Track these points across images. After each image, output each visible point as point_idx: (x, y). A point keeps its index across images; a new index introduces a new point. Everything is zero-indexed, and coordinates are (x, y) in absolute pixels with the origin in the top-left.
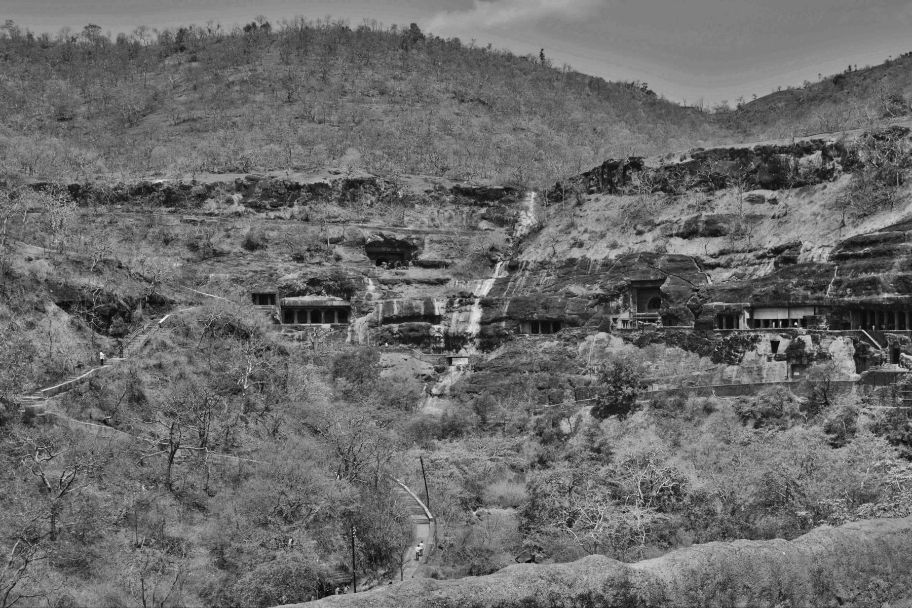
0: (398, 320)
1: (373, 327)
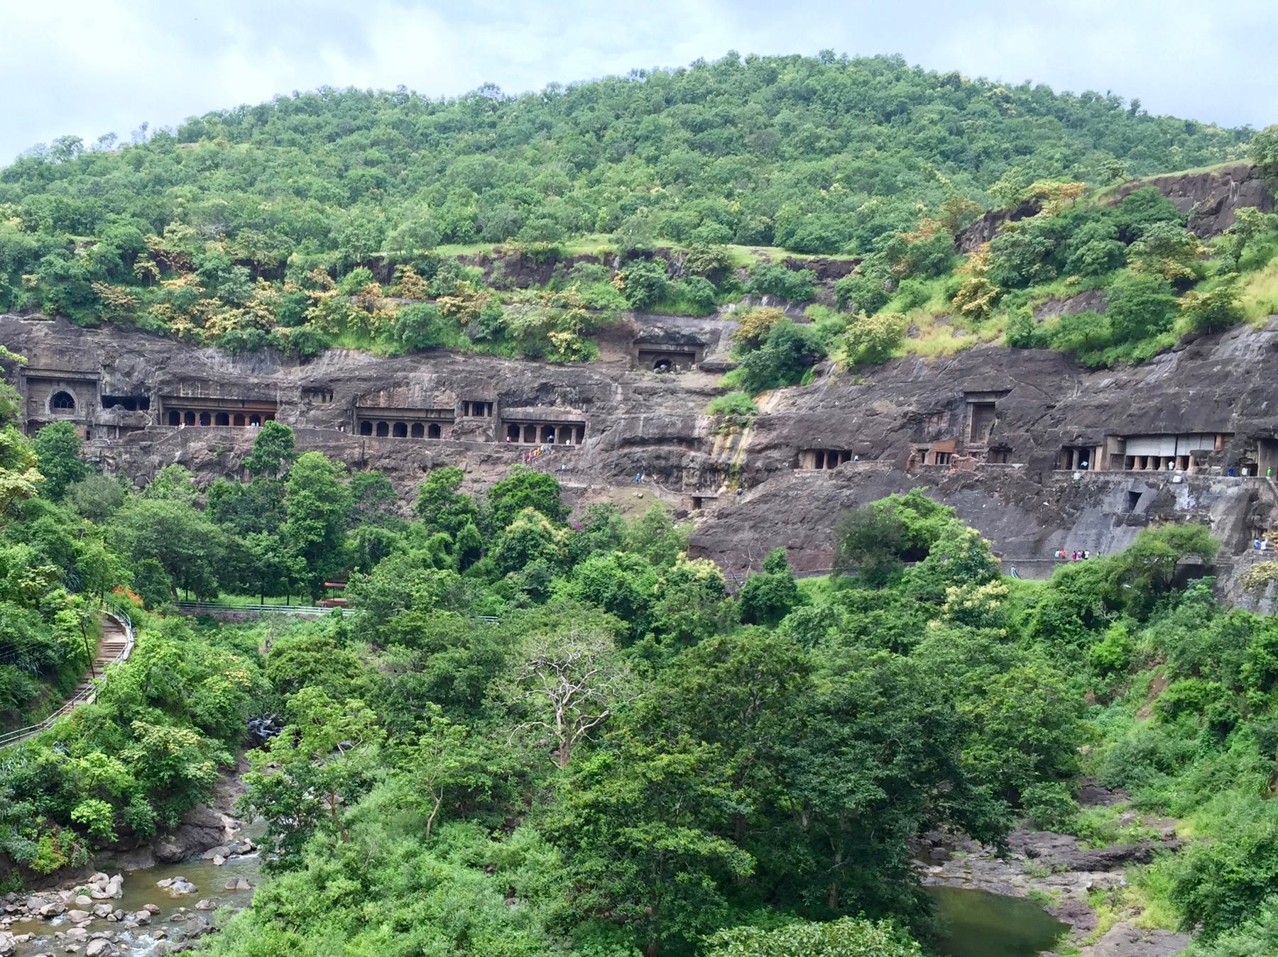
0: (643, 442)
1: (607, 451)
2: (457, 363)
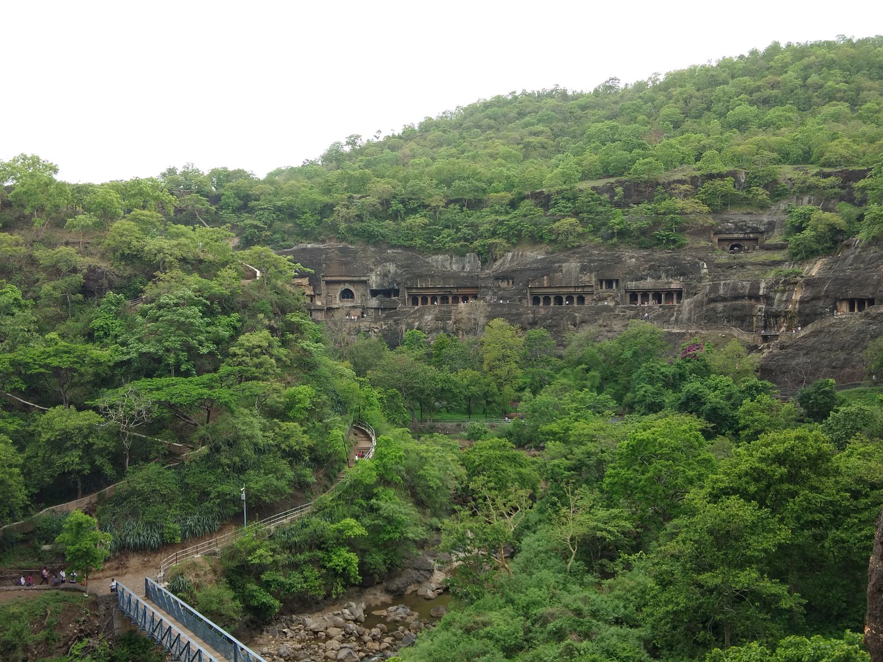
2: (594, 255)
